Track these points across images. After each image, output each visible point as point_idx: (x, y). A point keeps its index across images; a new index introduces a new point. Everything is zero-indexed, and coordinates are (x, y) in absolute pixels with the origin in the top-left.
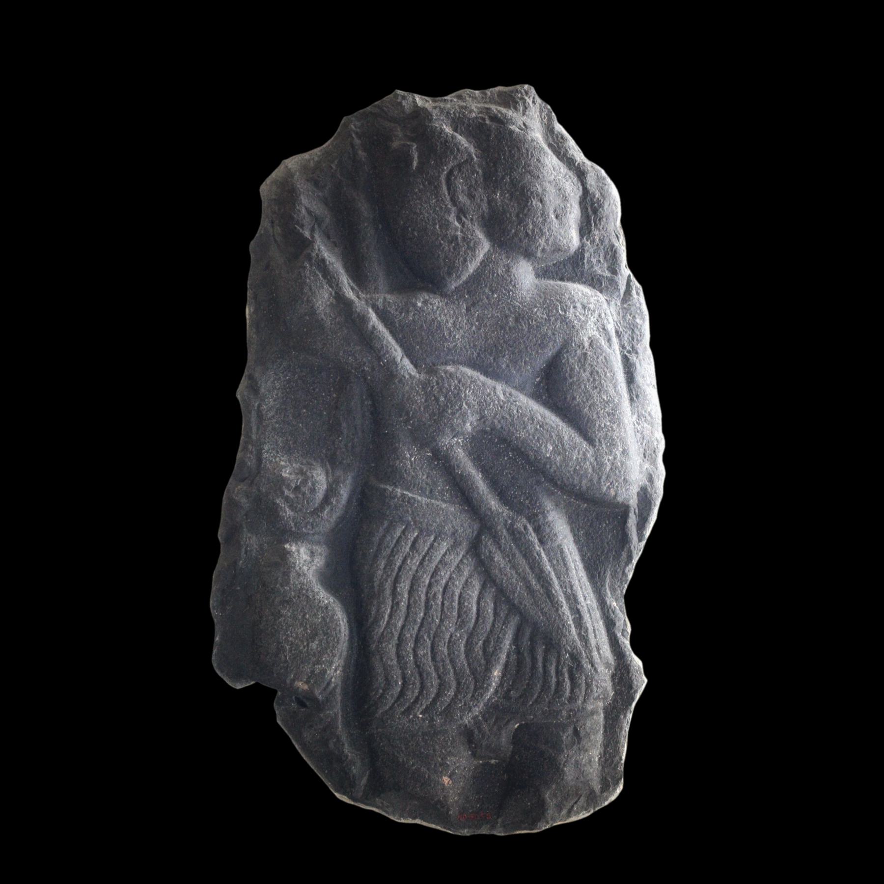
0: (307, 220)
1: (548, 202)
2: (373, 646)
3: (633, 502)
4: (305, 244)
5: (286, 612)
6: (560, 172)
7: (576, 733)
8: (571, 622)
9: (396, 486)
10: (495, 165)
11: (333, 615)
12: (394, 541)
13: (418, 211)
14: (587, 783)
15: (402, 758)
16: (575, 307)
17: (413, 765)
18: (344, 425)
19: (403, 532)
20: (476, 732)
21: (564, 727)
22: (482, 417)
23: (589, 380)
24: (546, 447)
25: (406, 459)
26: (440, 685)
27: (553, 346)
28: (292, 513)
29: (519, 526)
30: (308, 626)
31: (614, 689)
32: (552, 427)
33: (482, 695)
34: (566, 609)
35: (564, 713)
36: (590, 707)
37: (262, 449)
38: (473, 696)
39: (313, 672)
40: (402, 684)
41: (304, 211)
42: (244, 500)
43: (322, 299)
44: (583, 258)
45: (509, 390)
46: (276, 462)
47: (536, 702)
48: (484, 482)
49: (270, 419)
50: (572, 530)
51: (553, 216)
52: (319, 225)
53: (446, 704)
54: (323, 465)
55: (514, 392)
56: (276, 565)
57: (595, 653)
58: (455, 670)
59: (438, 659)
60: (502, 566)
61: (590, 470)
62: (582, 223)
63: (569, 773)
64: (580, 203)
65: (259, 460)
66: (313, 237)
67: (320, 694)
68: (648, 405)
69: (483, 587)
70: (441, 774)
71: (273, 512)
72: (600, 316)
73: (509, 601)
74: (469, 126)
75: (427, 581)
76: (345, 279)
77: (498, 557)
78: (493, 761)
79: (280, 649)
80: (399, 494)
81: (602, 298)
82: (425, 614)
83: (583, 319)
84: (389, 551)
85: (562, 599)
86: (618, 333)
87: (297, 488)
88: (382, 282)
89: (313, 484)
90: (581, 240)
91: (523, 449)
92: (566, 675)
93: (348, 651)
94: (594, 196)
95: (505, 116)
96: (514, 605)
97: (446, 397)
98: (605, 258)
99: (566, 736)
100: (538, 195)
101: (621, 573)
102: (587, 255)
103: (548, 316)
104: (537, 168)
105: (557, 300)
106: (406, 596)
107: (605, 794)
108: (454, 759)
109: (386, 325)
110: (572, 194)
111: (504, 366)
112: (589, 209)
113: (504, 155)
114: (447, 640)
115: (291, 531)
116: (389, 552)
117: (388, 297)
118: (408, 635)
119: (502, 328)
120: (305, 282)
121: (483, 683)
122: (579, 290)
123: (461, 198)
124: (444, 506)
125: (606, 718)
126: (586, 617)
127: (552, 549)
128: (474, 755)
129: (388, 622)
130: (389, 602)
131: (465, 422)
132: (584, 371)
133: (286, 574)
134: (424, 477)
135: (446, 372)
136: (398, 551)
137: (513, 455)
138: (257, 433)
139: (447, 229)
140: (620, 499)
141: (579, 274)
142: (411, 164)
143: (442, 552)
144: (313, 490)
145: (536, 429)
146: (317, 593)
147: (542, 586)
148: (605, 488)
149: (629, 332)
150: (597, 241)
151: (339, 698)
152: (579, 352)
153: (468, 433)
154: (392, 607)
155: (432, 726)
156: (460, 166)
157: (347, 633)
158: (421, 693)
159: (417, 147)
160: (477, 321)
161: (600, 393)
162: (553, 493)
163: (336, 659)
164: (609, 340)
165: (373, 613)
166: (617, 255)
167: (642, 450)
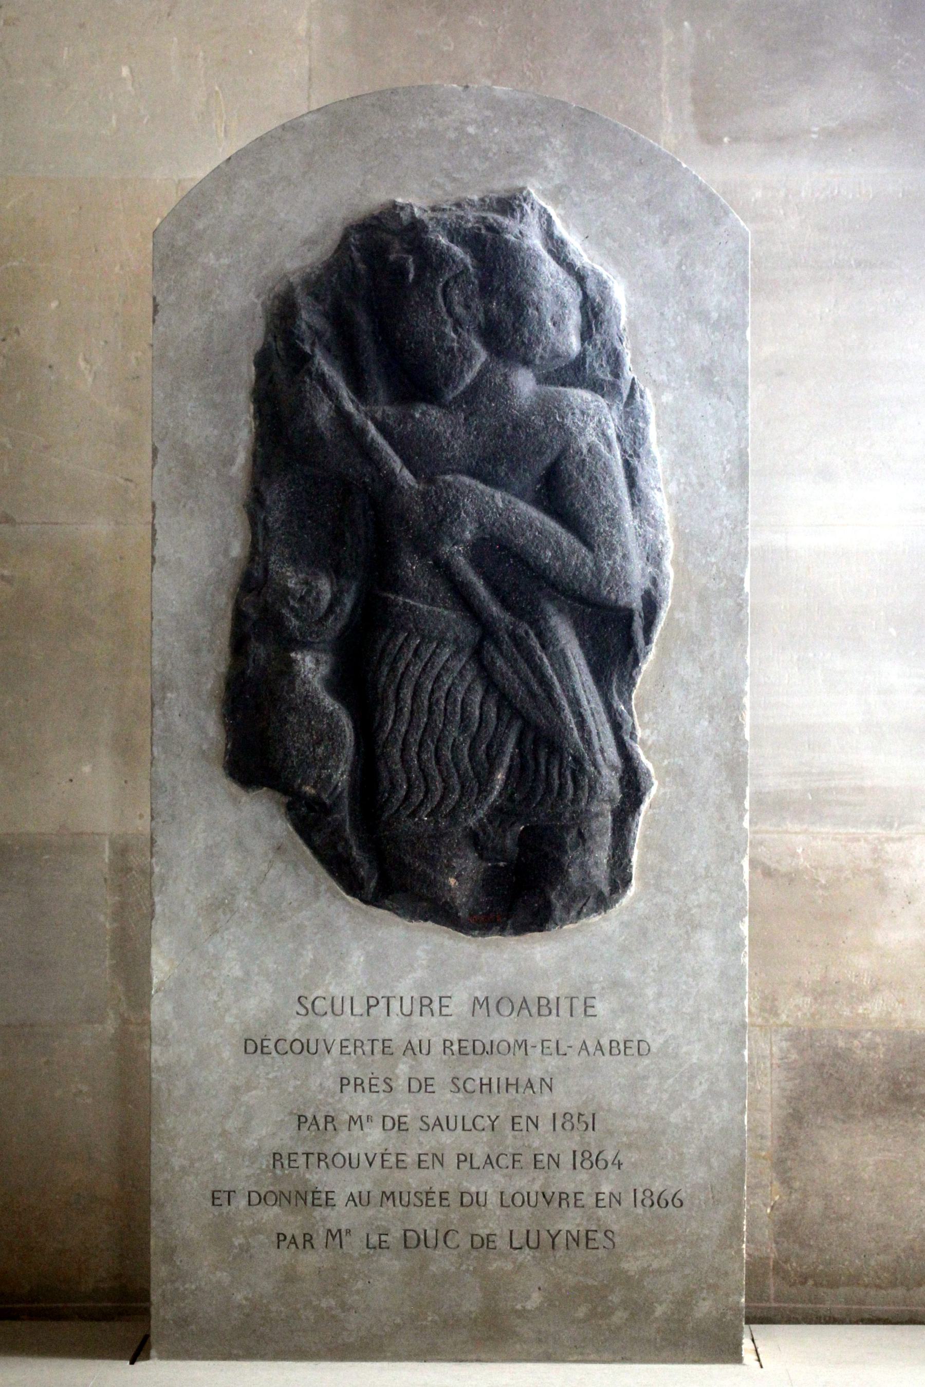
0: (307, 334)
1: (545, 310)
2: (379, 751)
3: (637, 604)
4: (307, 358)
5: (293, 718)
6: (559, 279)
7: (580, 835)
8: (573, 725)
9: (398, 595)
10: (491, 276)
11: (338, 722)
12: (397, 648)
13: (414, 323)
14: (593, 886)
15: (408, 859)
16: (573, 414)
17: (419, 866)
18: (347, 535)
19: (406, 639)
20: (481, 834)
21: (566, 828)
22: (481, 525)
23: (587, 486)
24: (545, 553)
25: (408, 567)
26: (445, 788)
27: (551, 453)
28: (297, 623)
29: (521, 632)
30: (314, 732)
31: (622, 792)
32: (550, 533)
33: (486, 798)
34: (568, 712)
35: (567, 815)
36: (594, 809)
37: (268, 560)
38: (477, 799)
39: (319, 777)
40: (408, 787)
41: (304, 326)
42: (251, 611)
43: (323, 413)
44: (584, 363)
45: (508, 497)
46: (282, 573)
47: (540, 803)
48: (486, 588)
49: (276, 531)
50: (577, 634)
51: (550, 324)
52: (320, 339)
53: (451, 807)
54: (329, 575)
55: (513, 499)
56: (282, 673)
57: (599, 757)
58: (459, 774)
59: (442, 763)
60: (504, 670)
61: (589, 575)
62: (583, 327)
63: (574, 875)
64: (581, 308)
65: (266, 570)
66: (313, 351)
67: (328, 798)
68: (652, 508)
69: (486, 691)
70: (448, 875)
71: (278, 622)
72: (600, 421)
73: (511, 706)
74: (465, 236)
75: (430, 687)
76: (344, 393)
77: (499, 662)
78: (502, 864)
79: (287, 755)
80: (401, 603)
81: (603, 402)
82: (428, 719)
83: (582, 425)
84: (391, 658)
85: (564, 703)
86: (619, 438)
87: (302, 599)
88: (381, 394)
89: (318, 594)
90: (582, 345)
91: (522, 556)
92: (569, 777)
93: (354, 757)
94: (595, 301)
95: (500, 225)
96: (516, 709)
97: (444, 506)
98: (608, 361)
99: (570, 838)
100: (534, 304)
101: (628, 677)
102: (588, 360)
103: (545, 423)
104: (533, 275)
105: (556, 408)
106: (409, 701)
107: (615, 896)
108: (461, 861)
109: (385, 438)
110: (571, 300)
111: (503, 474)
112: (590, 313)
113: (500, 265)
114: (450, 745)
115: (296, 639)
116: (392, 659)
117: (387, 408)
118: (412, 740)
119: (500, 436)
120: (305, 397)
121: (487, 785)
122: (580, 396)
123: (457, 308)
124: (446, 613)
125: (614, 820)
126: (590, 720)
127: (554, 653)
128: (481, 857)
129: (392, 728)
130: (393, 707)
131: (463, 531)
132: (583, 477)
133: (292, 682)
134: (426, 585)
135: (444, 482)
136: (400, 658)
137: (514, 561)
138: (264, 545)
139: (444, 341)
140: (621, 603)
141: (581, 379)
142: (408, 278)
143: (445, 658)
144: (317, 600)
145: (535, 536)
146: (323, 699)
147: (545, 690)
148: (605, 593)
149: (631, 436)
150: (599, 346)
151: (346, 801)
152: (577, 458)
153: (468, 541)
154: (396, 713)
155: (437, 828)
156: (455, 277)
157: (353, 738)
158: (425, 796)
159: (414, 260)
160: (475, 430)
161: (599, 498)
162: (556, 598)
163: (342, 764)
164: (609, 446)
165: (377, 718)
166: (621, 358)
167: (645, 554)
